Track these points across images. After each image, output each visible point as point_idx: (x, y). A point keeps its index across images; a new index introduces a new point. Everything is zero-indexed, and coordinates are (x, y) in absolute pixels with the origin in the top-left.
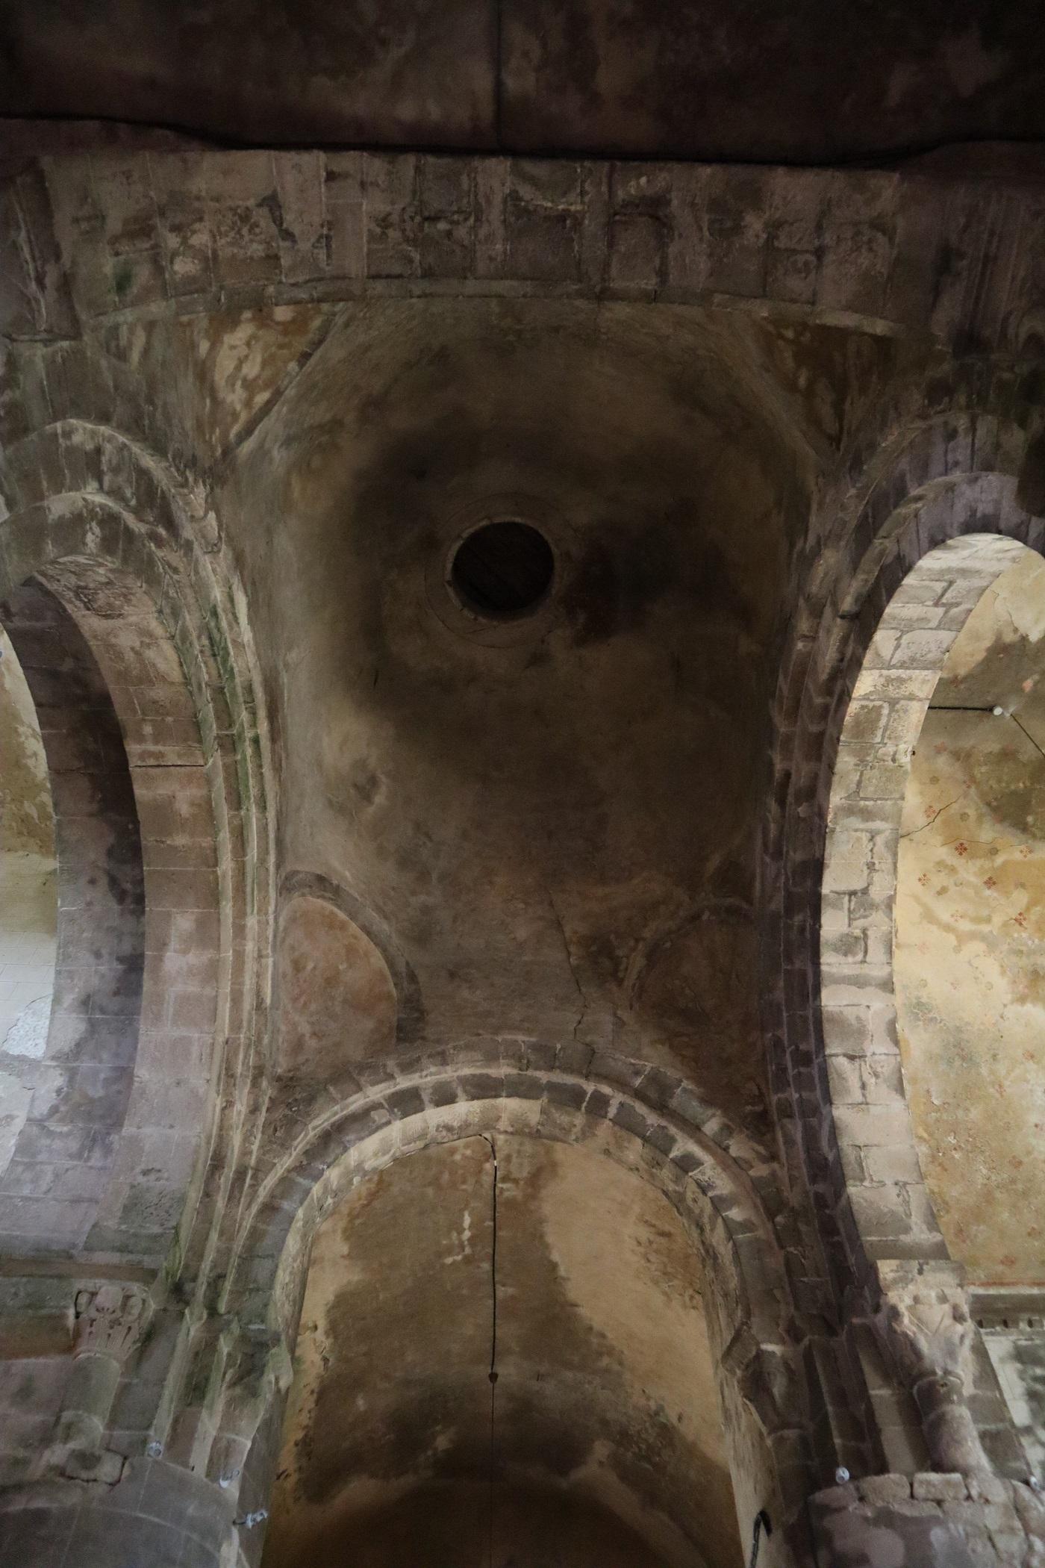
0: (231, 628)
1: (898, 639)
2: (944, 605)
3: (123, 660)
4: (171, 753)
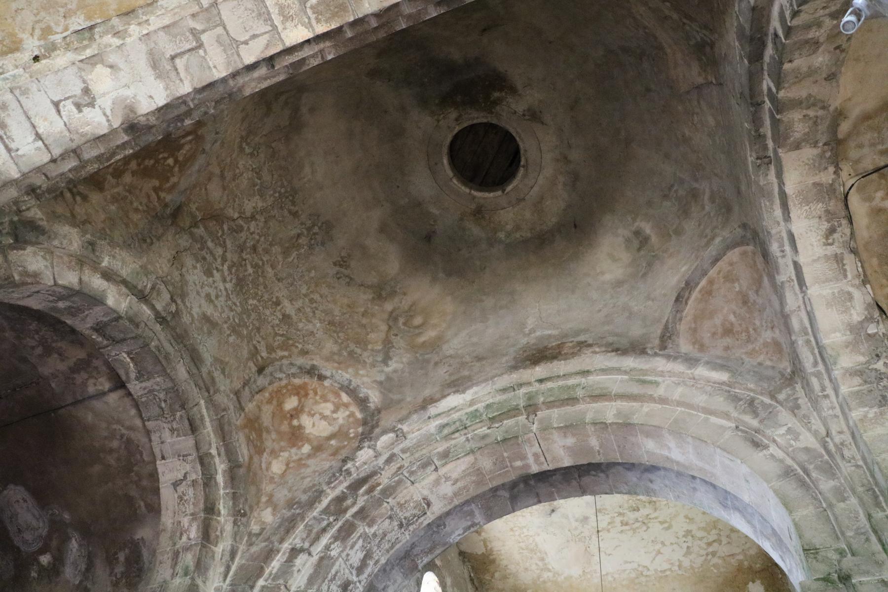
0: (459, 410)
1: (246, 43)
2: (198, 40)
3: (464, 488)
4: (530, 451)
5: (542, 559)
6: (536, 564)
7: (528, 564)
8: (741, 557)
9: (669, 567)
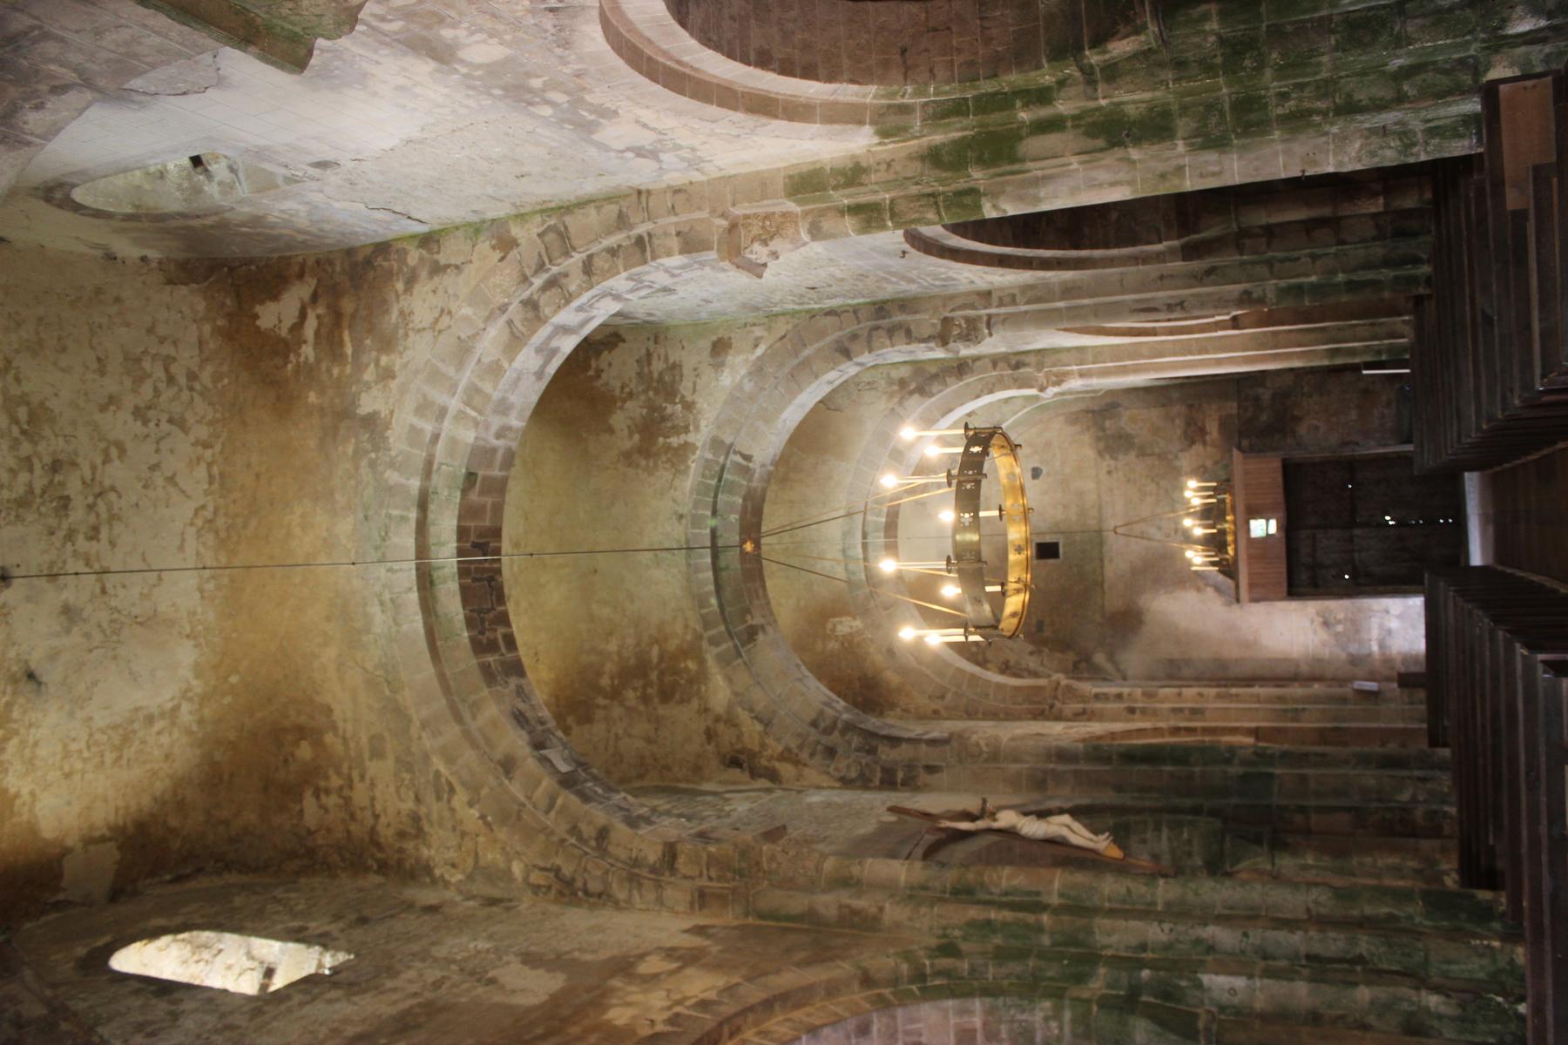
5: (150, 719)
6: (159, 733)
7: (156, 752)
8: (207, 328)
9: (203, 466)
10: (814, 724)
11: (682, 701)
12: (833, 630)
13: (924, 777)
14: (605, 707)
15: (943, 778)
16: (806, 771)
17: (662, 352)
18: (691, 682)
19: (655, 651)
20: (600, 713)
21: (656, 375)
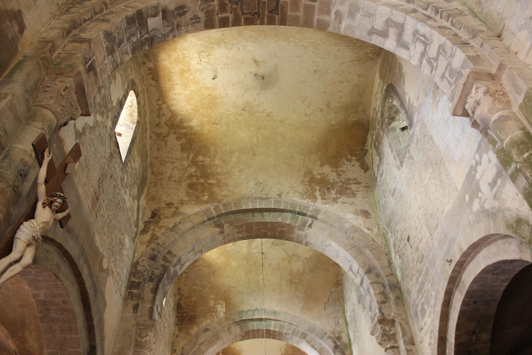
10: (169, 252)
11: (188, 193)
12: (219, 304)
13: (132, 303)
14: (188, 157)
15: (130, 313)
16: (145, 246)
17: (361, 189)
18: (197, 197)
19: (213, 181)
20: (185, 155)
21: (349, 186)
